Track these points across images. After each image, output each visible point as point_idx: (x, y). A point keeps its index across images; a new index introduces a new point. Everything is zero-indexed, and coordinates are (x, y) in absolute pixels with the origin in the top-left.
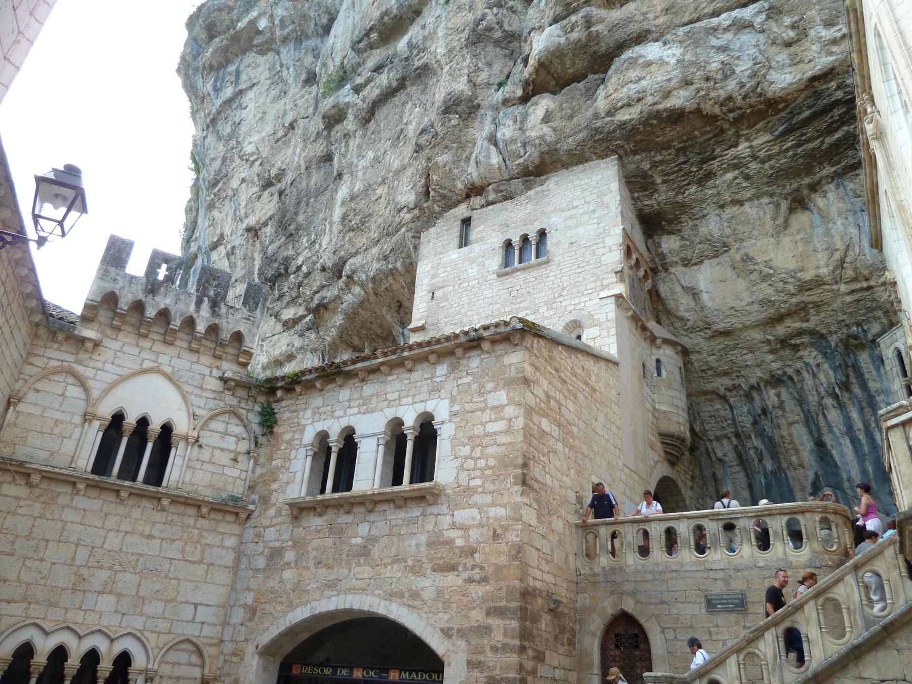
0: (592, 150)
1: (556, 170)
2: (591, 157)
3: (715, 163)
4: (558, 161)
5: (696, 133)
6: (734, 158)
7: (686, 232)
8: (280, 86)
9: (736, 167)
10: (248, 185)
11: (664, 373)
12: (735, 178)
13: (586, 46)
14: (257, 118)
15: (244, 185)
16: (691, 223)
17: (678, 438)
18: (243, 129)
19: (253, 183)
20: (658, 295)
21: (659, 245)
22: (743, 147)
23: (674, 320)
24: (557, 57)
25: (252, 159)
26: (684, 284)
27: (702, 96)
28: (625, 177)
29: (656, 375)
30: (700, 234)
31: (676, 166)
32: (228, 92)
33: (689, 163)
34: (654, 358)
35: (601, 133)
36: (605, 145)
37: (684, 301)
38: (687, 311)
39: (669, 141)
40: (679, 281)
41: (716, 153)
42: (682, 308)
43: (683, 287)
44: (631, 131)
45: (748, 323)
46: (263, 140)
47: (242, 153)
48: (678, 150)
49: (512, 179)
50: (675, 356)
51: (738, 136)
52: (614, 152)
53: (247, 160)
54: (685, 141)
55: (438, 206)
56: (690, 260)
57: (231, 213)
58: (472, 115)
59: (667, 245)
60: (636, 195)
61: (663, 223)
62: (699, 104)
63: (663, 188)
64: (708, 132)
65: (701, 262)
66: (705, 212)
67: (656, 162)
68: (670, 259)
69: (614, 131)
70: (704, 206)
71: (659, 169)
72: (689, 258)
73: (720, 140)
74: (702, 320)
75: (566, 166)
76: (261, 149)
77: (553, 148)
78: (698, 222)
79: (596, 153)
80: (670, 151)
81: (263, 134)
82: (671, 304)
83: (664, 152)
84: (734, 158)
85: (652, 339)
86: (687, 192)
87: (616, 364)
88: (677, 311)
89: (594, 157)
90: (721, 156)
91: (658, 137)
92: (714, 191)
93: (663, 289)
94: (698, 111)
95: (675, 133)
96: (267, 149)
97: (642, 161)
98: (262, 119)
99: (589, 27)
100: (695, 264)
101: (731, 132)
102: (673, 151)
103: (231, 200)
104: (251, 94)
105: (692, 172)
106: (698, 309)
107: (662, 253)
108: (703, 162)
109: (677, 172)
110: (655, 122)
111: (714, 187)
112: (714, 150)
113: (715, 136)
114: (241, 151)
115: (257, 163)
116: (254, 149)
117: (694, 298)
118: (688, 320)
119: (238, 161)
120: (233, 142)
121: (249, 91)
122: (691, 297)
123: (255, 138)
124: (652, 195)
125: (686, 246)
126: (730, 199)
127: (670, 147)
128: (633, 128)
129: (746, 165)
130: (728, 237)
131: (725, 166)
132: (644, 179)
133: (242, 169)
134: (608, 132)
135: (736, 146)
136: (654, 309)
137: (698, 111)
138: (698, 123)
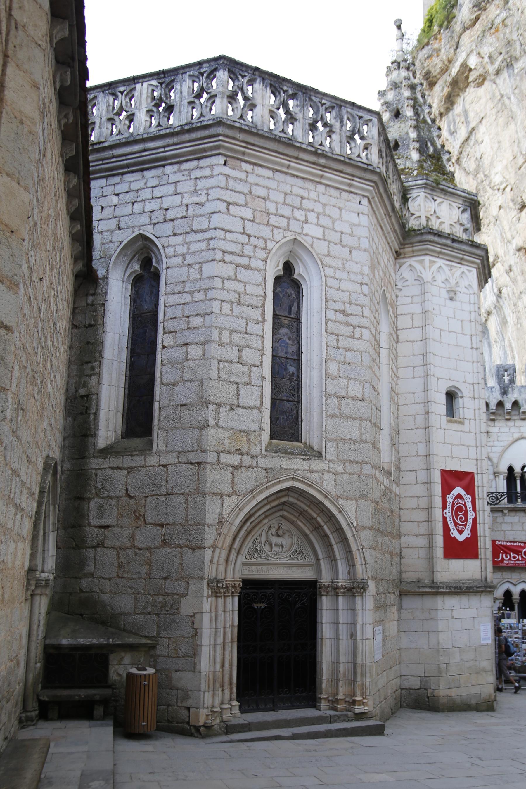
8: (505, 112)
10: (505, 210)
14: (495, 149)
15: (502, 210)
18: (486, 161)
19: (510, 208)
25: (502, 187)
32: (463, 133)
46: (506, 167)
47: (492, 185)
53: (498, 190)
57: (498, 236)
76: (507, 177)
81: (505, 162)
96: (512, 174)
98: (499, 148)
103: (495, 225)
104: (482, 129)
114: (490, 183)
115: (508, 189)
116: (501, 179)
119: (490, 191)
120: (481, 176)
121: (480, 126)
123: (499, 167)
133: (496, 198)
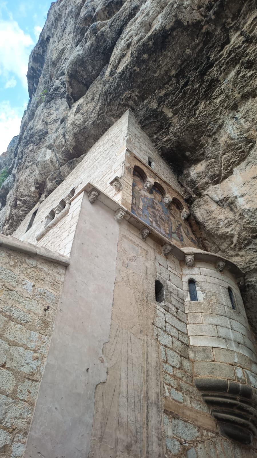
0: (109, 113)
1: (90, 146)
2: (111, 121)
3: (214, 71)
4: (89, 136)
5: (188, 51)
6: (230, 54)
7: (210, 151)
9: (234, 62)
11: (200, 295)
12: (238, 73)
13: (98, 47)
16: (210, 141)
17: (234, 391)
20: (198, 222)
21: (188, 175)
22: (235, 39)
23: (217, 242)
24: (80, 66)
26: (217, 199)
27: (177, 7)
28: (140, 123)
29: (189, 299)
30: (222, 145)
31: (180, 92)
33: (190, 83)
34: (186, 279)
35: (110, 93)
36: (117, 103)
37: (222, 217)
38: (228, 225)
39: (166, 72)
40: (212, 198)
41: (211, 59)
42: (222, 224)
43: (216, 202)
44: (130, 77)
48: (177, 76)
49: (61, 166)
50: (218, 275)
51: (226, 31)
52: (126, 106)
54: (181, 65)
55: (22, 211)
56: (220, 175)
58: (43, 140)
59: (195, 172)
60: (155, 137)
61: (187, 154)
62: (176, 16)
63: (175, 120)
64: (198, 44)
65: (231, 173)
66: (220, 121)
67: (161, 98)
68: (200, 182)
69: (118, 85)
70: (217, 117)
71: (166, 103)
72: (217, 173)
73: (211, 45)
74: (245, 229)
75: (96, 139)
77: (82, 127)
78: (217, 136)
79: (113, 115)
80: (171, 82)
82: (210, 225)
83: (166, 86)
84: (230, 54)
85: (181, 259)
86: (197, 112)
87: (65, 266)
88: (217, 229)
89: (113, 120)
90: (216, 60)
91: (155, 72)
92: (223, 97)
93: (199, 213)
94: (178, 23)
95: (167, 60)
97: (149, 103)
99: (96, 33)
100: (225, 177)
101: (218, 32)
102: (174, 80)
105: (195, 90)
106: (237, 218)
107: (192, 180)
108: (203, 74)
109: (183, 97)
110: (145, 56)
111: (221, 94)
112: (208, 58)
113: (206, 43)
117: (231, 209)
118: (232, 236)
122: (228, 210)
124: (168, 130)
125: (212, 163)
126: (239, 96)
127: (170, 78)
128: (131, 73)
129: (244, 54)
130: (248, 130)
131: (224, 66)
132: (157, 117)
134: (115, 89)
135: (228, 41)
136: (198, 239)
137: (178, 23)
138: (184, 39)
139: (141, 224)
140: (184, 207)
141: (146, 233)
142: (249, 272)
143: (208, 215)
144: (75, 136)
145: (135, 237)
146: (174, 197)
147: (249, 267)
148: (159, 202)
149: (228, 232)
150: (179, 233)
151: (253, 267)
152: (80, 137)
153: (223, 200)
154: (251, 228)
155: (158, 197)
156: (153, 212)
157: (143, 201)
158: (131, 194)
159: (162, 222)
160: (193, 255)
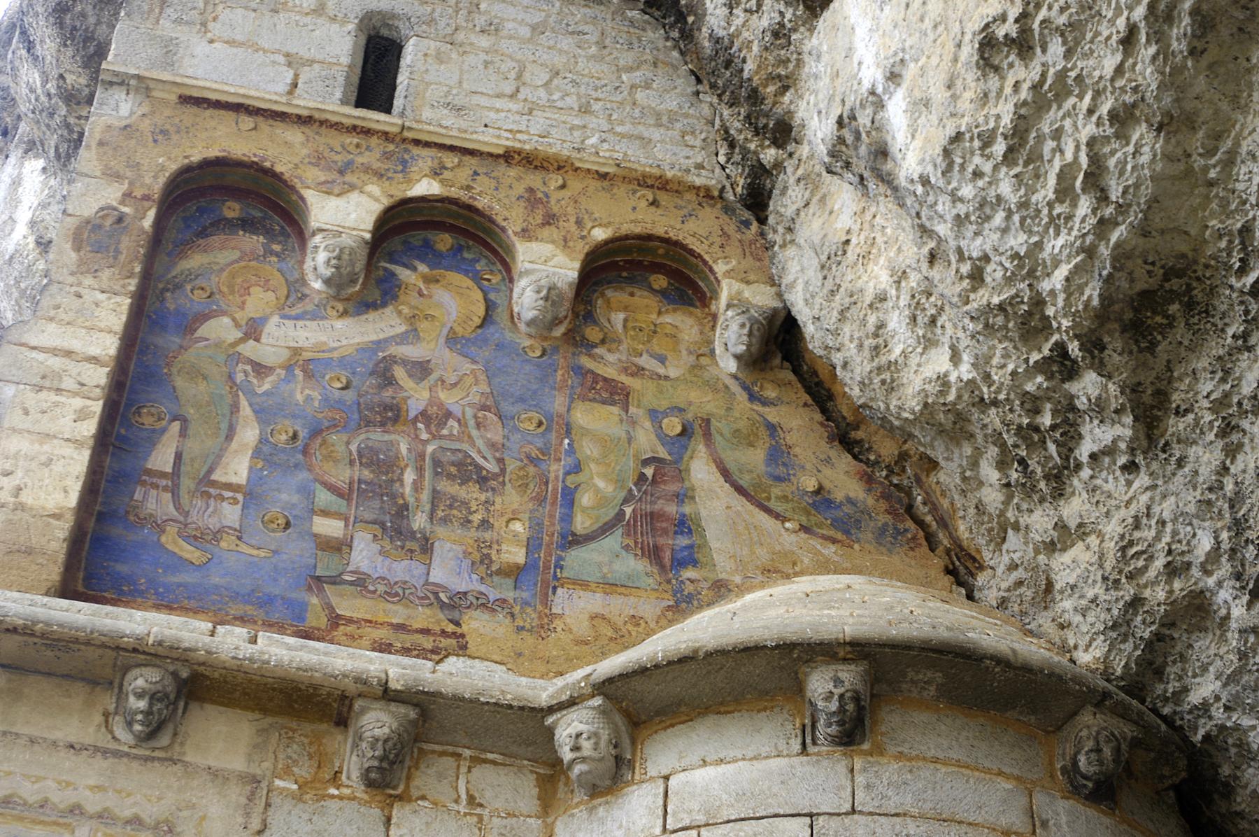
45: (1146, 72)
139: (93, 654)
140: (720, 268)
141: (140, 696)
142: (1158, 637)
143: (829, 284)
144: (60, 24)
145: (68, 761)
146: (600, 234)
147: (1136, 602)
148: (453, 340)
149: (943, 380)
150: (653, 517)
151: (1161, 595)
152: (92, 20)
153: (841, 140)
154: (1001, 307)
155: (452, 299)
156: (368, 457)
157: (261, 413)
158: (89, 428)
159: (472, 493)
160: (597, 701)
